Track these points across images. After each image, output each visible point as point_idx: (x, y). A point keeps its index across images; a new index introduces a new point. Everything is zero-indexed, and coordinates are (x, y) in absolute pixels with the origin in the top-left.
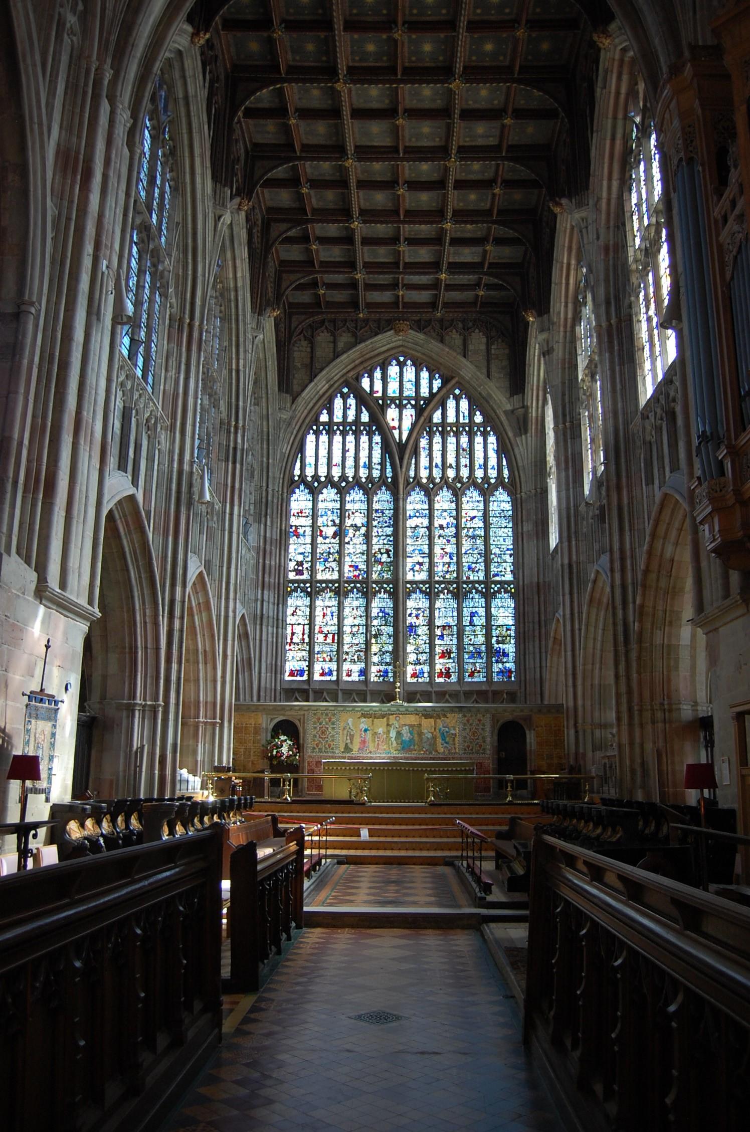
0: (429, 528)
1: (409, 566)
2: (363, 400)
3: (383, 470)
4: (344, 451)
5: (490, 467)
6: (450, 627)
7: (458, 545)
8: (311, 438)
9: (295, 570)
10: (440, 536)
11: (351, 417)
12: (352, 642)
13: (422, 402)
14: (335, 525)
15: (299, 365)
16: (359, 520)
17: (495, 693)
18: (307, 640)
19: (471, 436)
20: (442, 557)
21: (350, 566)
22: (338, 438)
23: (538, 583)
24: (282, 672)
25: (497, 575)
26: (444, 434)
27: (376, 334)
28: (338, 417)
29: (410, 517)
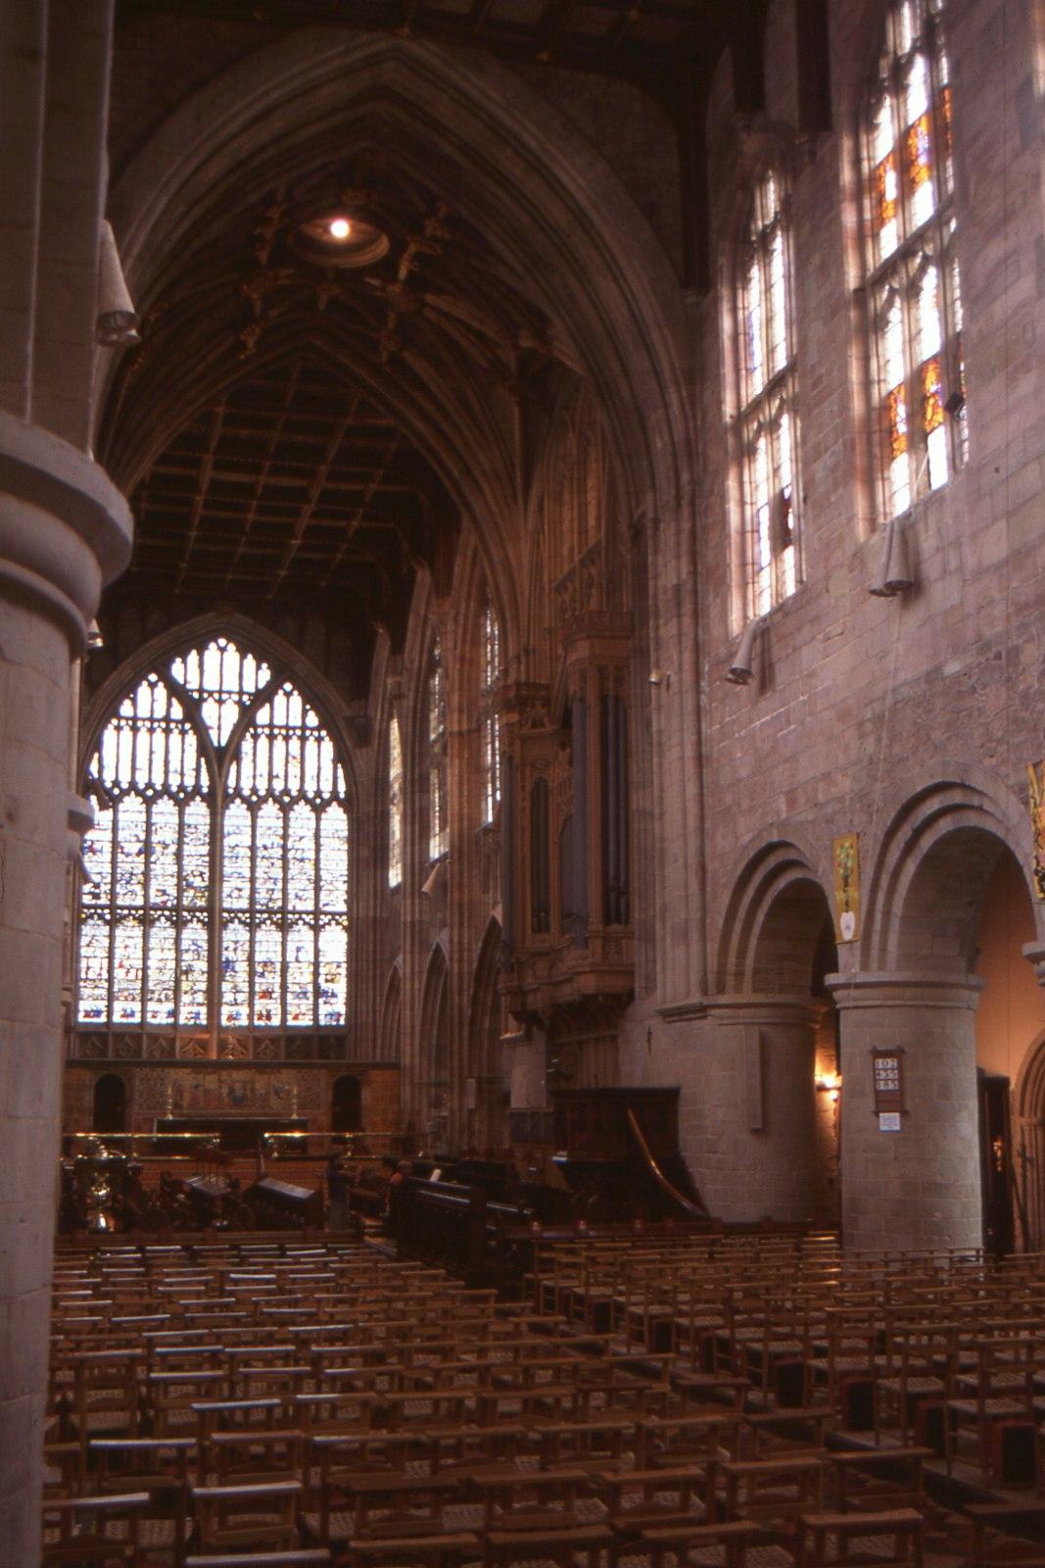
0: (253, 848)
2: (176, 690)
3: (198, 777)
6: (272, 963)
7: (285, 868)
8: (109, 735)
9: (90, 893)
10: (263, 857)
11: (160, 713)
13: (245, 698)
14: (139, 841)
18: (105, 976)
19: (303, 739)
20: (265, 881)
21: (158, 890)
23: (375, 918)
25: (327, 904)
26: (271, 738)
29: (229, 834)
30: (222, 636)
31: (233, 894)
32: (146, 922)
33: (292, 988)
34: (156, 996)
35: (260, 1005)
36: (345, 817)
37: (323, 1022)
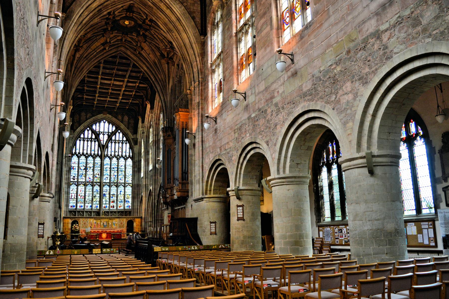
0: (110, 168)
1: (104, 178)
2: (93, 132)
4: (88, 146)
5: (127, 152)
7: (118, 173)
8: (78, 142)
11: (90, 137)
12: (88, 198)
14: (84, 166)
15: (76, 121)
16: (91, 165)
17: (126, 212)
18: (76, 198)
19: (122, 143)
20: (113, 176)
22: (86, 142)
24: (69, 206)
26: (115, 143)
27: (98, 115)
28: (86, 137)
30: (105, 119)
31: (106, 180)
32: (85, 185)
33: (119, 200)
34: (87, 202)
35: (112, 204)
36: (131, 161)
37: (126, 208)
